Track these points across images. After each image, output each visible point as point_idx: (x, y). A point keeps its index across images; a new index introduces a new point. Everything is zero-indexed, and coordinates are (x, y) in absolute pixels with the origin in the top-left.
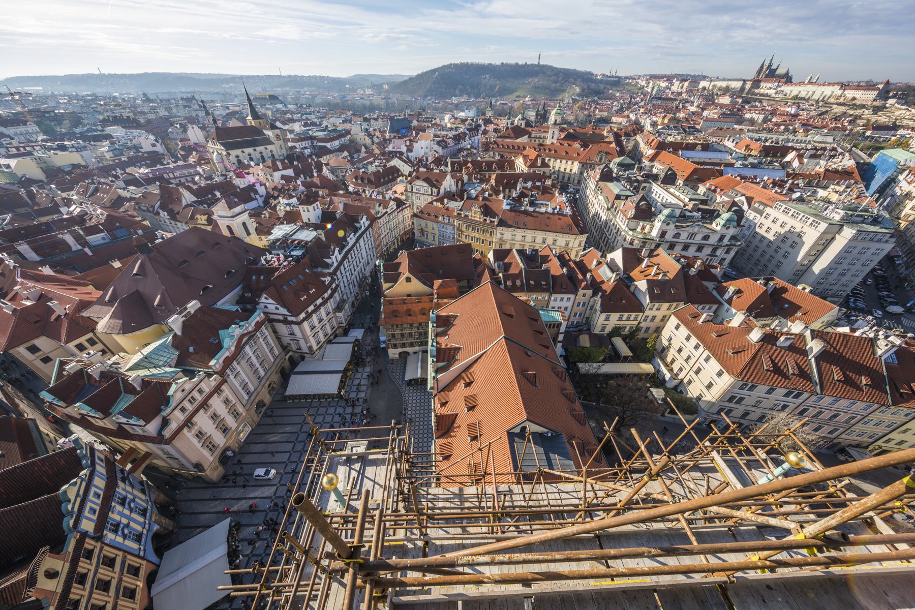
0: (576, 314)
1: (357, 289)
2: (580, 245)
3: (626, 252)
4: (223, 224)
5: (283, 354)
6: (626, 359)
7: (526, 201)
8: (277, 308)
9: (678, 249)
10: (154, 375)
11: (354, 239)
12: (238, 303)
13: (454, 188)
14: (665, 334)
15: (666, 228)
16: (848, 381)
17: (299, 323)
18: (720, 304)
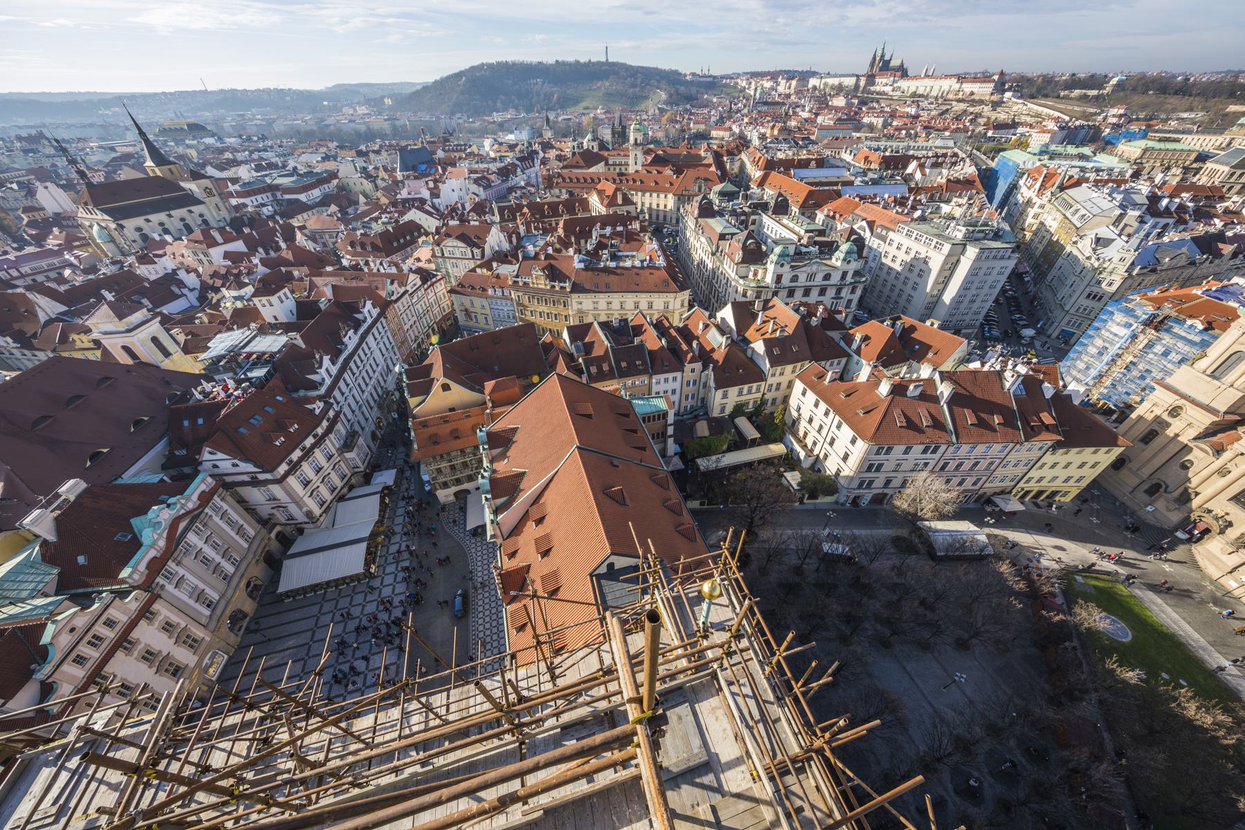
0: (687, 397)
1: (376, 412)
2: (682, 305)
3: (737, 307)
4: (114, 345)
5: (264, 531)
6: (754, 443)
7: (605, 254)
8: (235, 465)
9: (799, 294)
10: (11, 617)
11: (356, 339)
12: (164, 468)
13: (506, 246)
14: (793, 402)
15: (781, 271)
16: (982, 424)
17: (280, 481)
18: (849, 356)
